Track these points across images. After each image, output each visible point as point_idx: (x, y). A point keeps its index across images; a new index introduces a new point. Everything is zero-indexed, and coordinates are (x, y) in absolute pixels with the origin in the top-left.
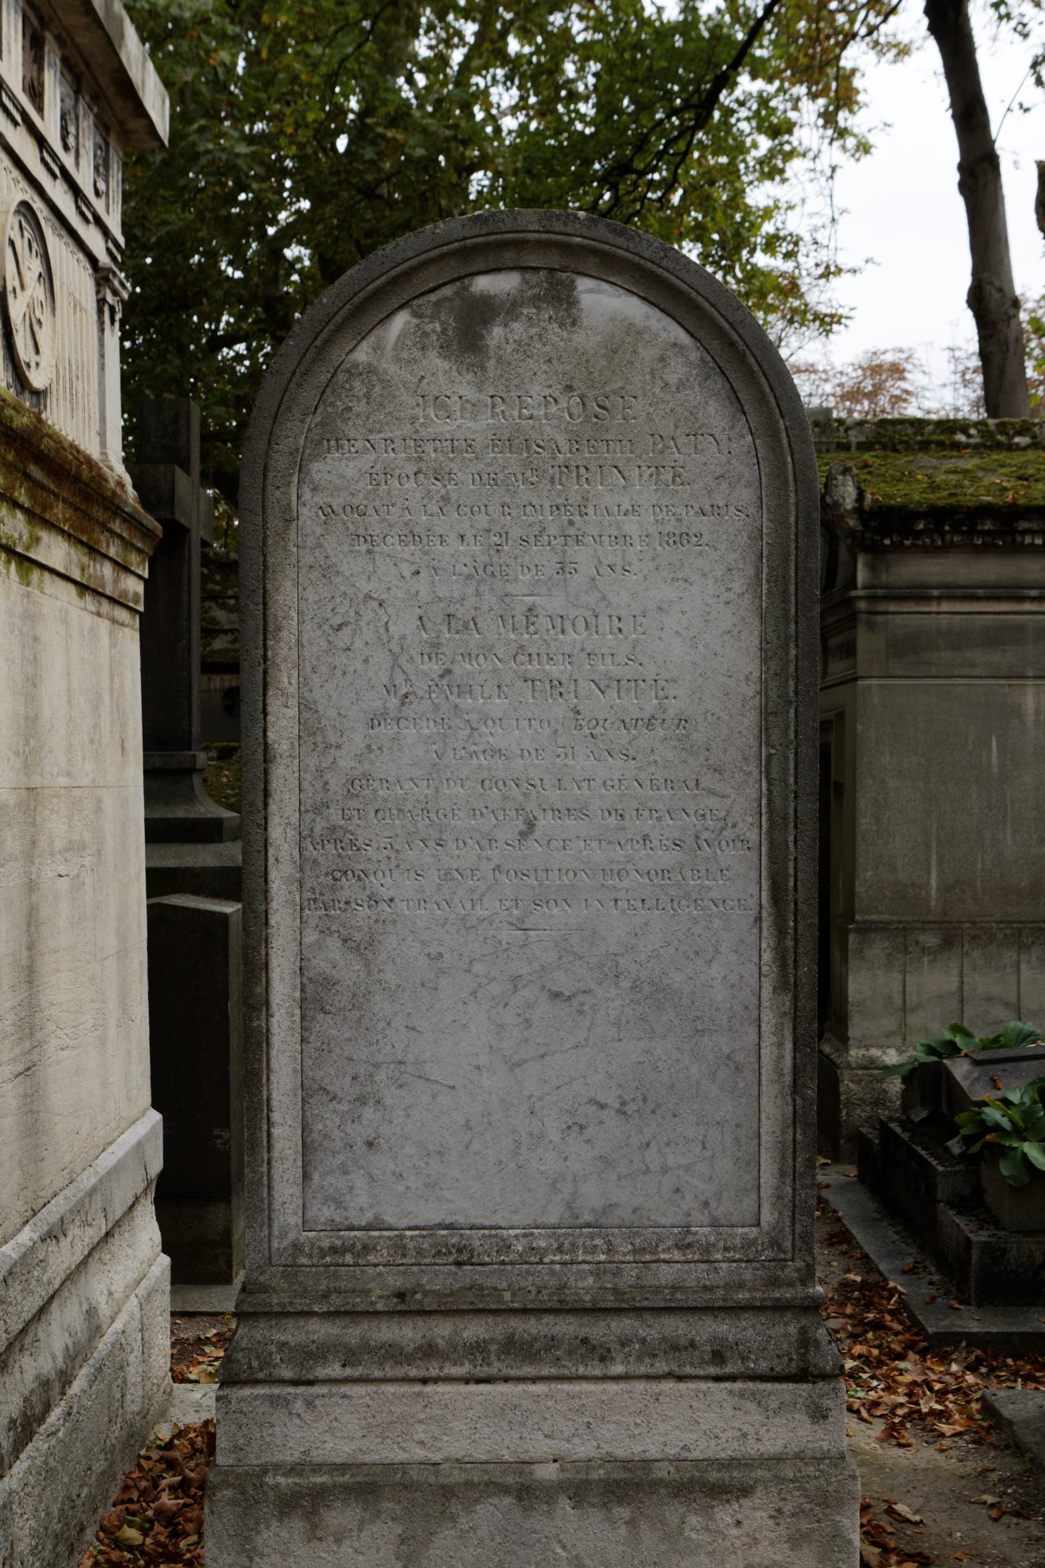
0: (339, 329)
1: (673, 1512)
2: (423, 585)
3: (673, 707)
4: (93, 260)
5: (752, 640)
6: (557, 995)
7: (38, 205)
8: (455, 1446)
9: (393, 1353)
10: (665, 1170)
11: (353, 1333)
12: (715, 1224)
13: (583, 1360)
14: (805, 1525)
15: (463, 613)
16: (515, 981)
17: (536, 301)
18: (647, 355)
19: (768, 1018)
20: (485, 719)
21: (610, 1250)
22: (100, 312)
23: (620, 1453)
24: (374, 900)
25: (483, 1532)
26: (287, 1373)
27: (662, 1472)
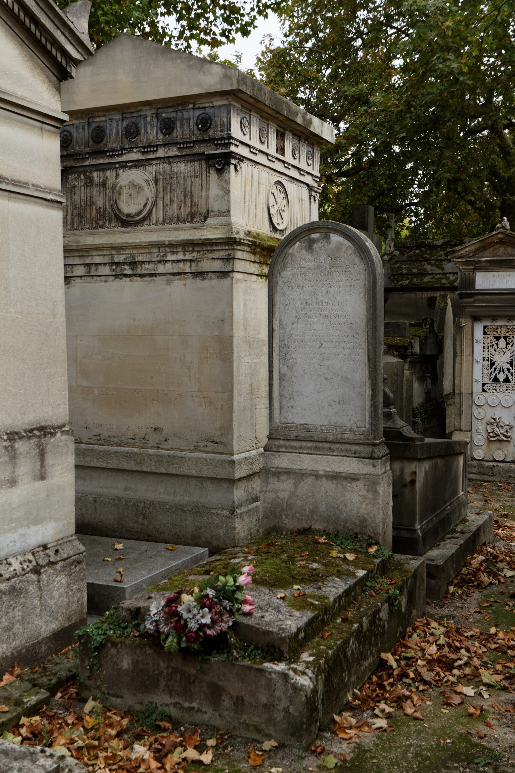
0: (286, 246)
1: (344, 483)
2: (302, 296)
3: (349, 320)
4: (307, 185)
5: (364, 307)
6: (327, 379)
7: (284, 180)
8: (305, 467)
9: (294, 447)
10: (347, 415)
11: (288, 443)
12: (357, 427)
13: (329, 451)
14: (370, 488)
15: (309, 302)
16: (319, 375)
17: (322, 239)
18: (344, 249)
19: (367, 385)
20: (313, 323)
21: (336, 430)
22: (310, 199)
23: (336, 471)
24: (293, 359)
25: (309, 483)
26: (275, 450)
27: (342, 475)
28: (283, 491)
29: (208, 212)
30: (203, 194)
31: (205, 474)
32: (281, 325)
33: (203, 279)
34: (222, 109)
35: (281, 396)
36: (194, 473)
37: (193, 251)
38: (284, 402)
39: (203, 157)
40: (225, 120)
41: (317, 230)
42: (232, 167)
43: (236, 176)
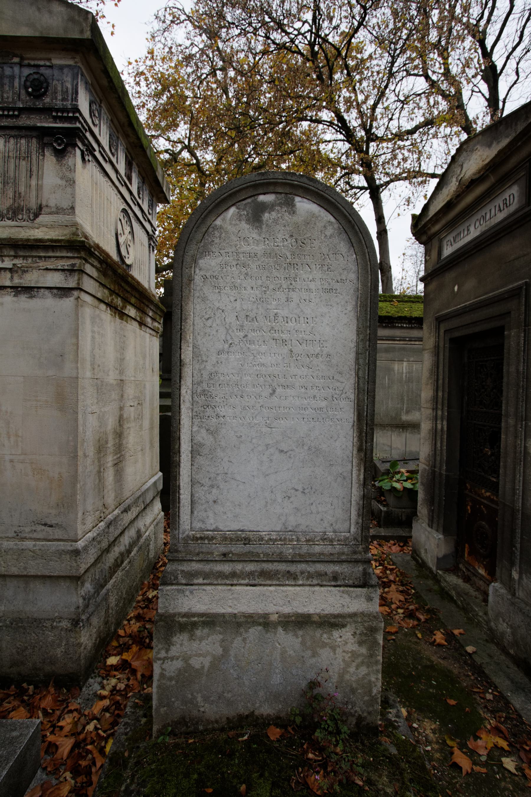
0: (210, 212)
2: (238, 304)
3: (326, 351)
6: (282, 451)
9: (221, 575)
10: (318, 513)
11: (207, 568)
12: (335, 531)
13: (288, 579)
14: (364, 638)
15: (252, 315)
16: (267, 446)
17: (280, 205)
22: (149, 247)
23: (300, 611)
24: (218, 416)
26: (184, 582)
28: (200, 655)
29: (40, 208)
30: (34, 182)
31: (32, 572)
32: (196, 355)
33: (31, 297)
34: (66, 70)
35: (193, 483)
36: (14, 570)
37: (16, 257)
38: (200, 493)
39: (34, 134)
40: (69, 86)
41: (271, 188)
42: (78, 152)
43: (84, 167)
